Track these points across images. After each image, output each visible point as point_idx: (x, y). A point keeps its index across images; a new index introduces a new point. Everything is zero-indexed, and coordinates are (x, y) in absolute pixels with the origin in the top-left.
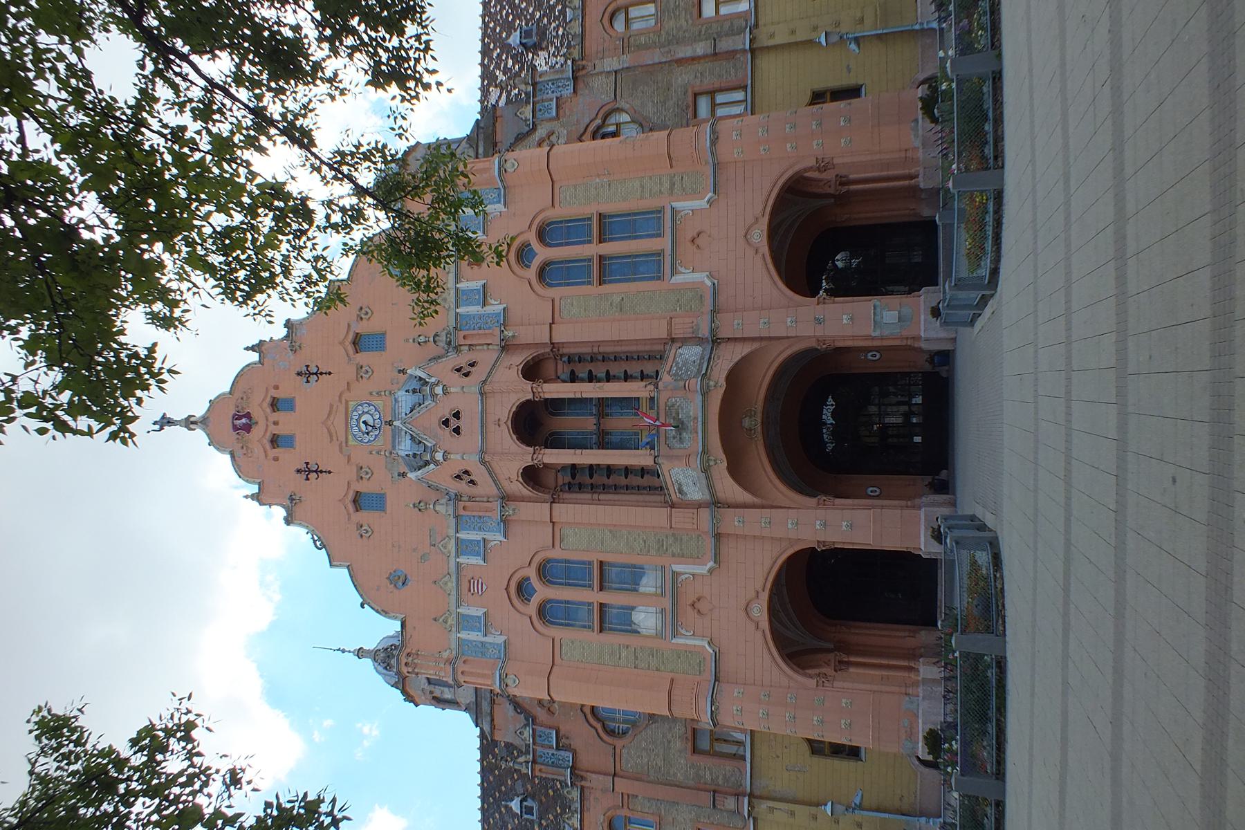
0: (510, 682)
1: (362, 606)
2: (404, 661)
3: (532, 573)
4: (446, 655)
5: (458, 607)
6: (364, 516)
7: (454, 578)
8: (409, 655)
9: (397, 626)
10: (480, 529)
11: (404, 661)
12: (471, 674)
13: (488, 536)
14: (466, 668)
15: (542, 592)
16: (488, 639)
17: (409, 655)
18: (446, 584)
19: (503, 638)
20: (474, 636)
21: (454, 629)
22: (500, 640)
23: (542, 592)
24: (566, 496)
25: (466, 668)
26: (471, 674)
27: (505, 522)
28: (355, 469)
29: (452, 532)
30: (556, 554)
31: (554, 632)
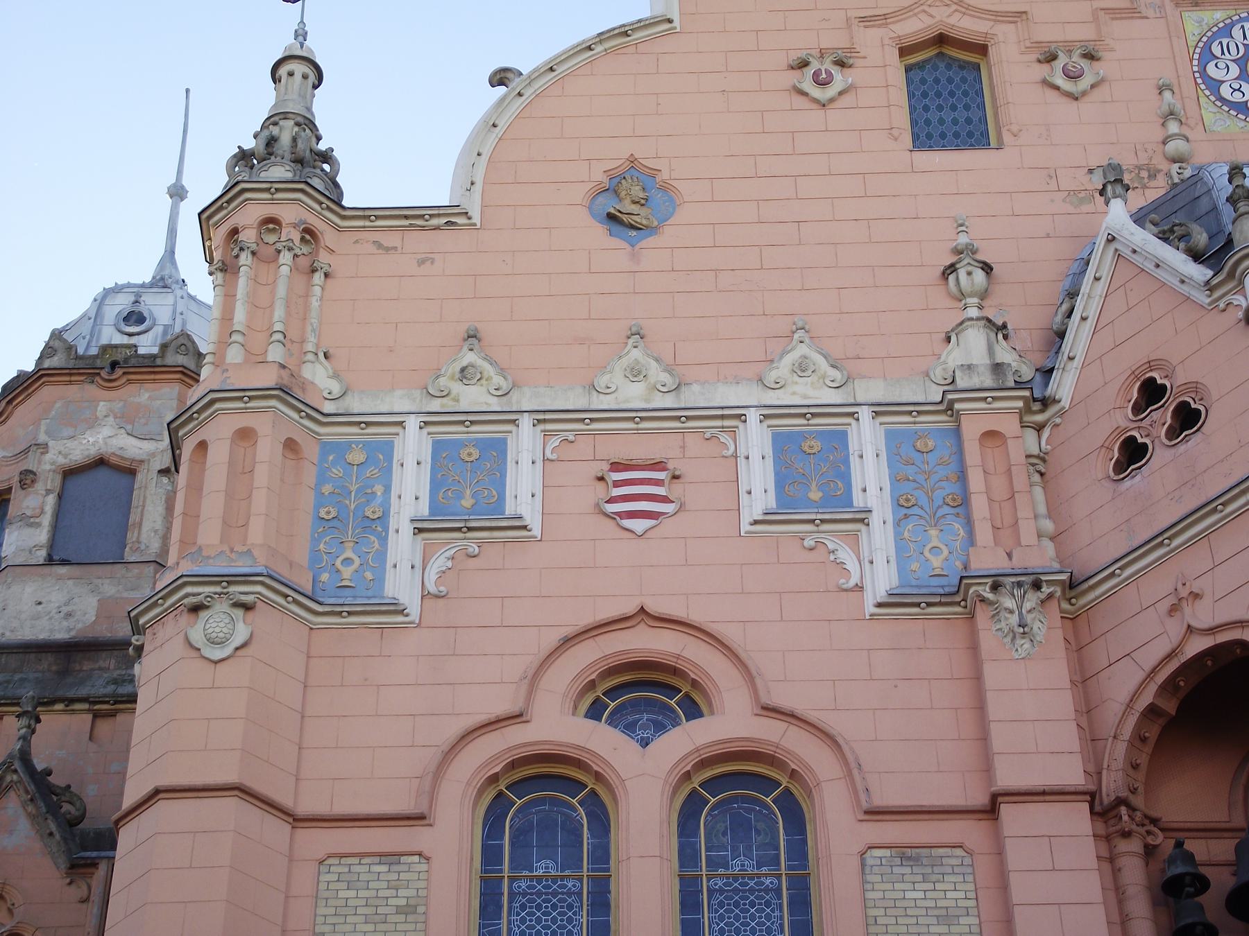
0: (217, 619)
1: (500, 78)
2: (290, 213)
3: (729, 722)
4: (319, 376)
5: (542, 417)
6: (882, 88)
7: (669, 401)
8: (309, 234)
9: (433, 188)
10: (903, 507)
11: (290, 213)
12: (241, 472)
13: (881, 536)
14: (267, 449)
15: (644, 776)
16: (402, 545)
17: (309, 234)
18: (636, 373)
19: (410, 598)
20: (410, 491)
21: (436, 405)
22: (401, 585)
23: (644, 776)
24: (1134, 872)
25: (267, 449)
26: (241, 472)
27: (960, 597)
28: (1084, 33)
29: (875, 390)
30: (837, 831)
31: (454, 838)
